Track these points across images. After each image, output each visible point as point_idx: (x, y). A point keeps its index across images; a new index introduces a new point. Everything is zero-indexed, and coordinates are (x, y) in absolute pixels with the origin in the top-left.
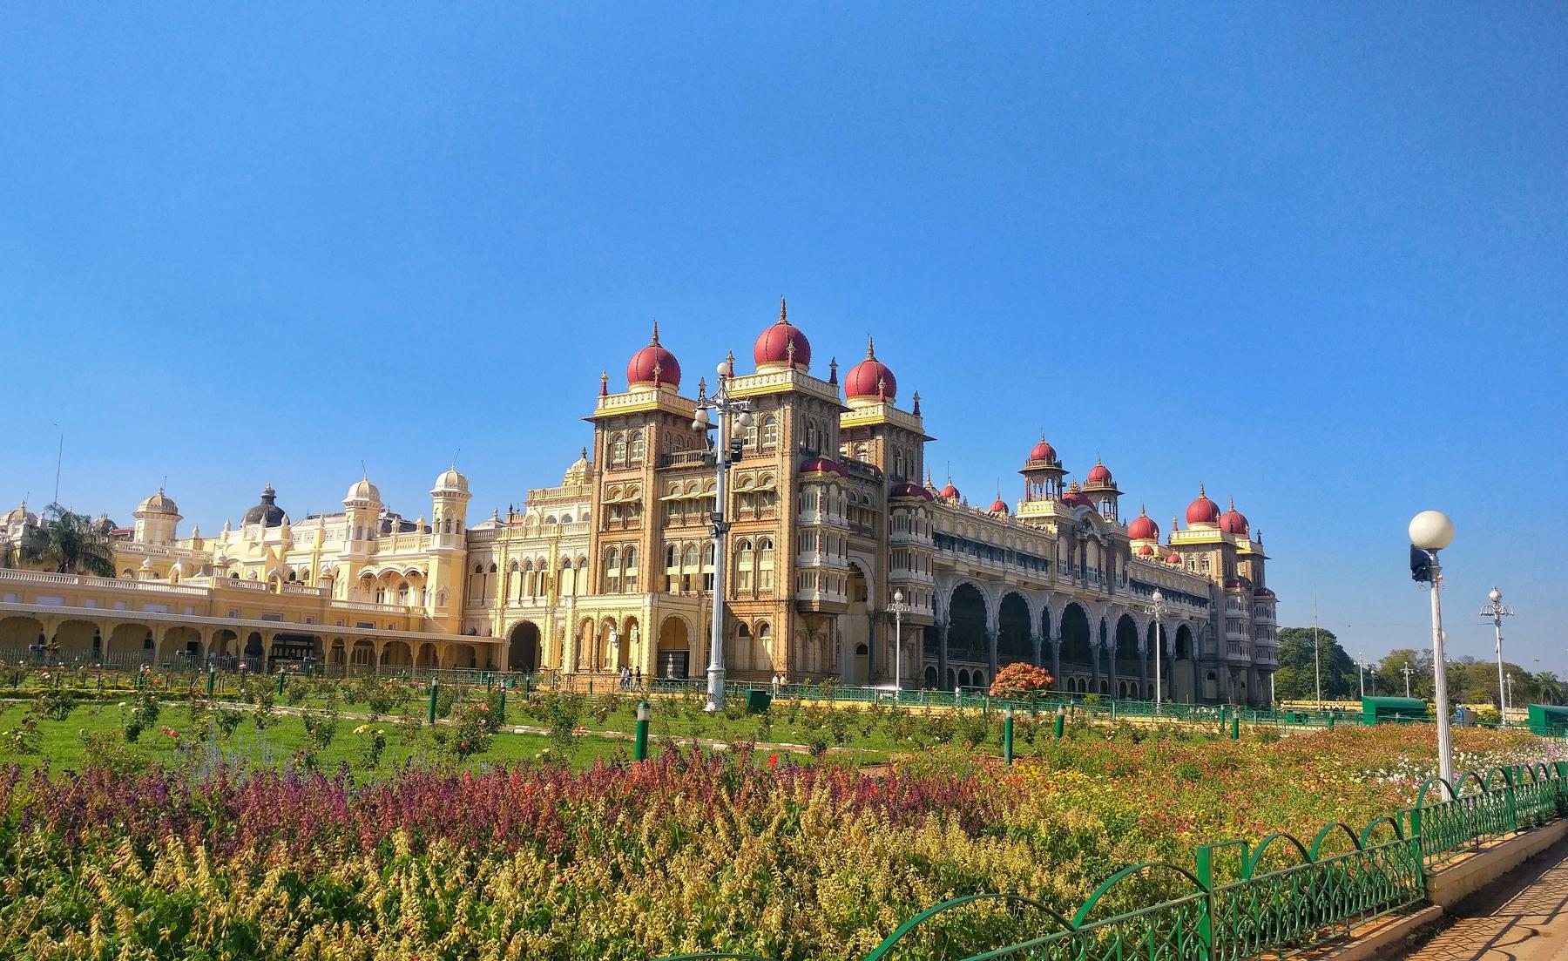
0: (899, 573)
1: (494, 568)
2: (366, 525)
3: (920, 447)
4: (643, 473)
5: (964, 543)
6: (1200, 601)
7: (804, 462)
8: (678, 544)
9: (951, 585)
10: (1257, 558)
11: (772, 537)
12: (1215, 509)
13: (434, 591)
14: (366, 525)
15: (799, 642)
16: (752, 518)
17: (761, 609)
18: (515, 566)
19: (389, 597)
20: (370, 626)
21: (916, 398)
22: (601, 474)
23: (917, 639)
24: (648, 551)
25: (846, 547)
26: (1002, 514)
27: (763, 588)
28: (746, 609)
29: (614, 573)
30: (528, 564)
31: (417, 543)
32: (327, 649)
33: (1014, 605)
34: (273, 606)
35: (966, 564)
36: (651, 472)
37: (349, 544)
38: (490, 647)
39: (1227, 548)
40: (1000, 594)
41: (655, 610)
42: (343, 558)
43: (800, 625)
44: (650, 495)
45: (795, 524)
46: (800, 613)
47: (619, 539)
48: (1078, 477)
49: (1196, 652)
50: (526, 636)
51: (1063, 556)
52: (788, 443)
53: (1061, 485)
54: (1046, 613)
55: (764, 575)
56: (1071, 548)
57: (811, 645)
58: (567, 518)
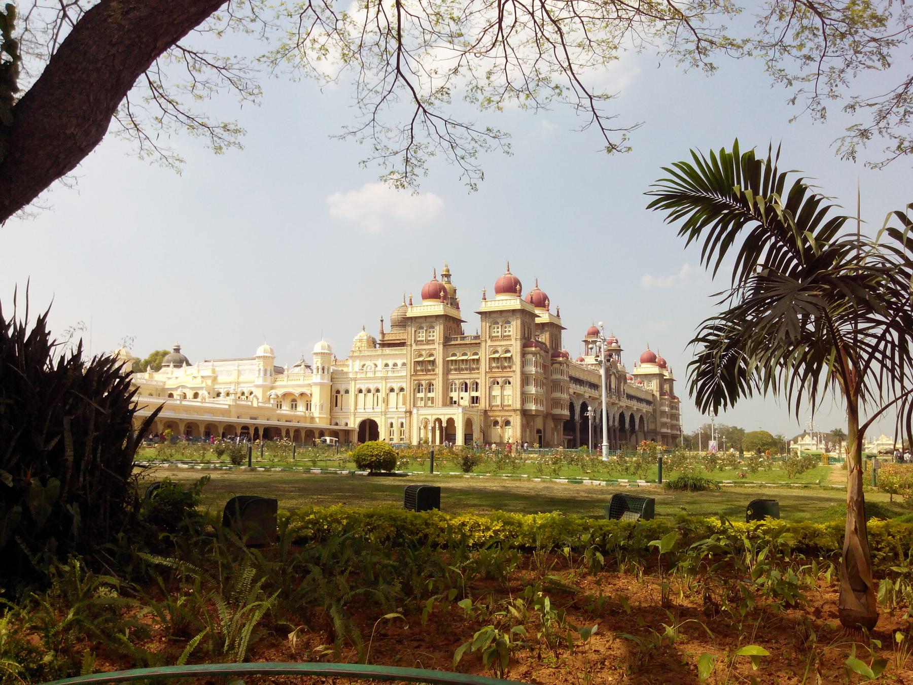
0: (557, 395)
1: (347, 392)
2: (269, 369)
3: (560, 332)
4: (436, 346)
6: (648, 403)
8: (457, 382)
10: (671, 381)
11: (511, 380)
12: (655, 357)
13: (318, 404)
17: (507, 414)
18: (361, 391)
22: (411, 345)
24: (441, 384)
27: (506, 403)
28: (497, 413)
30: (369, 391)
31: (302, 378)
33: (584, 407)
34: (254, 413)
36: (441, 346)
37: (261, 379)
38: (347, 433)
39: (661, 376)
40: (581, 402)
41: (464, 414)
42: (258, 386)
44: (441, 357)
47: (424, 379)
52: (519, 334)
55: (506, 397)
58: (376, 365)
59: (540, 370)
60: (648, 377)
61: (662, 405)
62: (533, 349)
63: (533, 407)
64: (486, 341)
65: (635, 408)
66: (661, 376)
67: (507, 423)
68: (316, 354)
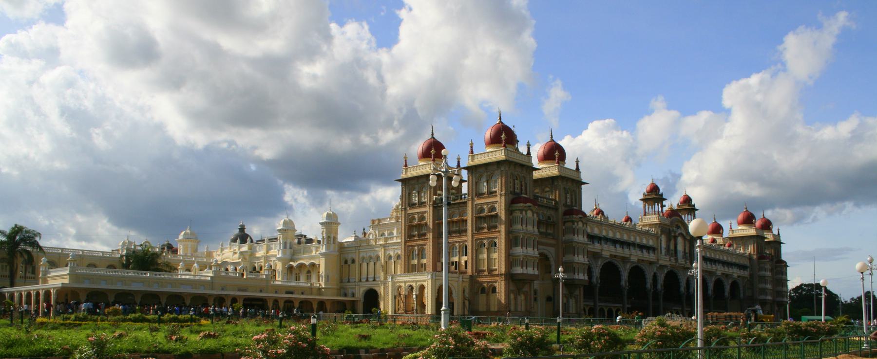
0: (568, 258)
1: (353, 261)
2: (288, 242)
4: (427, 209)
5: (607, 240)
7: (514, 200)
9: (600, 263)
11: (496, 240)
14: (288, 242)
15: (512, 296)
16: (486, 230)
17: (492, 279)
19: (303, 278)
20: (292, 293)
21: (577, 162)
23: (579, 292)
25: (537, 244)
26: (628, 223)
29: (415, 262)
32: (270, 304)
35: (608, 251)
40: (628, 266)
43: (512, 288)
45: (508, 232)
46: (513, 280)
48: (673, 202)
49: (742, 295)
50: (372, 298)
51: (664, 245)
53: (662, 206)
54: (655, 277)
56: (668, 241)
57: (519, 297)
59: (532, 229)
60: (743, 240)
61: (760, 269)
62: (522, 204)
63: (519, 270)
64: (473, 200)
65: (719, 273)
66: (758, 239)
67: (494, 290)
68: (322, 224)
